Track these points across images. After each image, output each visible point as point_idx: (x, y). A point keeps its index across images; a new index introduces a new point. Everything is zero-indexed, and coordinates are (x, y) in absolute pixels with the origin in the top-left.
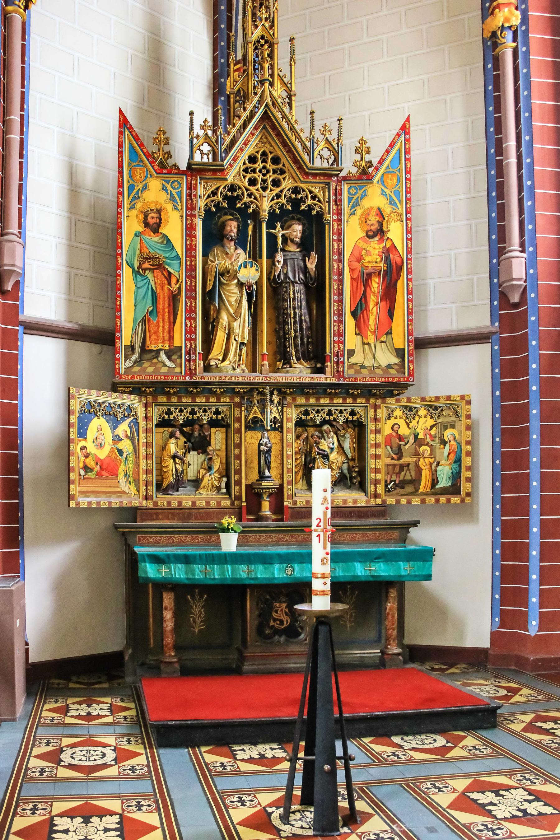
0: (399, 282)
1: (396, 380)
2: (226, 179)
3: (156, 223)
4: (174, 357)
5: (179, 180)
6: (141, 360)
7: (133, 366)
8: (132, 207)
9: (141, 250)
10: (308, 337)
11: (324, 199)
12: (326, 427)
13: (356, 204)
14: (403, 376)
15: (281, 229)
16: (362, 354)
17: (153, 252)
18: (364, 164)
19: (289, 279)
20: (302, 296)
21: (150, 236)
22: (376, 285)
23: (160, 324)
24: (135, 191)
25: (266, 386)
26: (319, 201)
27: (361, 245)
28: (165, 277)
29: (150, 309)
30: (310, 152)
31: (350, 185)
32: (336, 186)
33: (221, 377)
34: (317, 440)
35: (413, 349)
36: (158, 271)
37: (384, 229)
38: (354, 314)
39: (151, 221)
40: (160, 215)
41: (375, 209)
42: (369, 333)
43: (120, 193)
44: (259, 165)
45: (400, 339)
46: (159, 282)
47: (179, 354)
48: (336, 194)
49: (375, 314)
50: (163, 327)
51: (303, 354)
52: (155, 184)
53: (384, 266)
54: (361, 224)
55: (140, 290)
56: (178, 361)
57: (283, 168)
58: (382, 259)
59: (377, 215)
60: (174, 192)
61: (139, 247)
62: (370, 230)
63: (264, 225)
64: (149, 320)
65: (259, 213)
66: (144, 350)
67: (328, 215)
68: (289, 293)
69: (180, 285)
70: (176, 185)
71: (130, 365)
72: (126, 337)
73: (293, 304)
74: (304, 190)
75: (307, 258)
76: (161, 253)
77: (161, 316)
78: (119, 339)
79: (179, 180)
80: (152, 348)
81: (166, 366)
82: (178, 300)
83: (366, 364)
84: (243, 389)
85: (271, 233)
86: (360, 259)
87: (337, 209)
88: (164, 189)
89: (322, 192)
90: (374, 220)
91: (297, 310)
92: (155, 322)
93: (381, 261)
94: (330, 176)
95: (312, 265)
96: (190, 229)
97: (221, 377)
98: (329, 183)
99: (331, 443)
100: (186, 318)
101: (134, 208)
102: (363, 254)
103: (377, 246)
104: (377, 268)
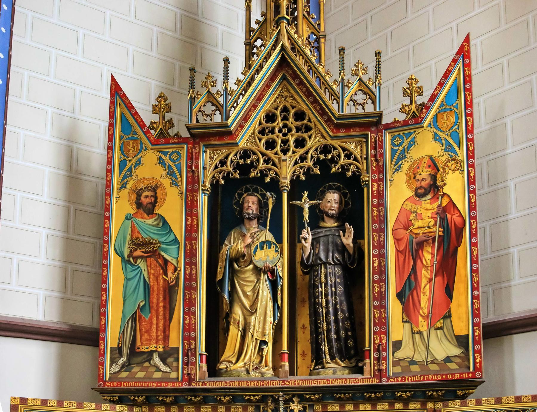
0: (460, 249)
1: (457, 377)
2: (236, 144)
3: (151, 203)
4: (170, 360)
5: (179, 150)
6: (130, 364)
7: (120, 371)
8: (123, 187)
9: (132, 235)
10: (346, 331)
11: (361, 157)
13: (402, 157)
14: (468, 371)
15: (307, 199)
16: (411, 346)
17: (147, 236)
18: (414, 108)
19: (320, 259)
20: (338, 280)
21: (143, 218)
22: (428, 256)
23: (153, 320)
24: (128, 167)
25: (280, 392)
26: (356, 159)
27: (408, 208)
28: (160, 265)
29: (142, 304)
30: (339, 98)
31: (393, 134)
32: (376, 138)
33: (226, 382)
35: (479, 335)
36: (152, 259)
37: (439, 183)
38: (400, 296)
39: (145, 201)
40: (156, 193)
41: (427, 160)
42: (420, 319)
43: (109, 171)
44: (279, 123)
45: (462, 323)
46: (153, 272)
47: (176, 356)
48: (375, 148)
49: (427, 293)
50: (157, 324)
51: (339, 351)
52: (150, 157)
53: (439, 231)
54: (408, 182)
55: (130, 283)
56: (175, 364)
57: (309, 124)
58: (436, 222)
59: (429, 167)
60: (172, 165)
61: (129, 232)
62: (421, 187)
63: (285, 196)
64: (140, 317)
65: (279, 181)
66: (133, 352)
67: (365, 175)
68: (321, 277)
69: (179, 274)
70: (175, 157)
71: (117, 370)
72: (111, 339)
73: (325, 290)
74: (335, 148)
75: (341, 232)
76: (155, 237)
77: (154, 312)
78: (104, 339)
79: (179, 150)
80: (143, 350)
81: (160, 370)
82: (176, 292)
83: (417, 358)
84: (254, 396)
85: (295, 205)
86: (407, 226)
87: (378, 165)
88: (161, 162)
89: (359, 148)
90: (425, 173)
91: (330, 298)
92: (147, 319)
93: (435, 224)
94: (367, 126)
95: (348, 240)
96: (191, 208)
97: (226, 382)
98: (367, 135)
100: (185, 313)
101: (125, 187)
102: (411, 218)
103: (429, 206)
104: (430, 235)
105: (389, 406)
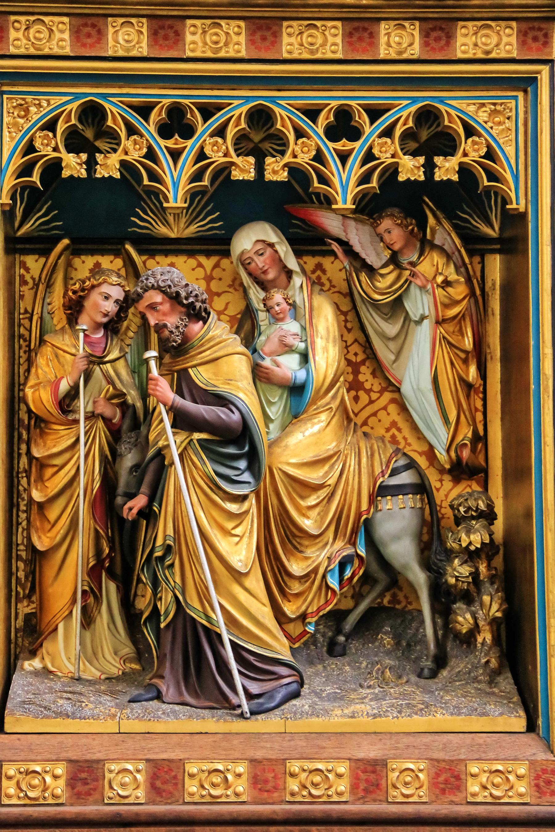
12: (252, 238)
34: (172, 321)
99: (288, 349)
105: (348, 36)
